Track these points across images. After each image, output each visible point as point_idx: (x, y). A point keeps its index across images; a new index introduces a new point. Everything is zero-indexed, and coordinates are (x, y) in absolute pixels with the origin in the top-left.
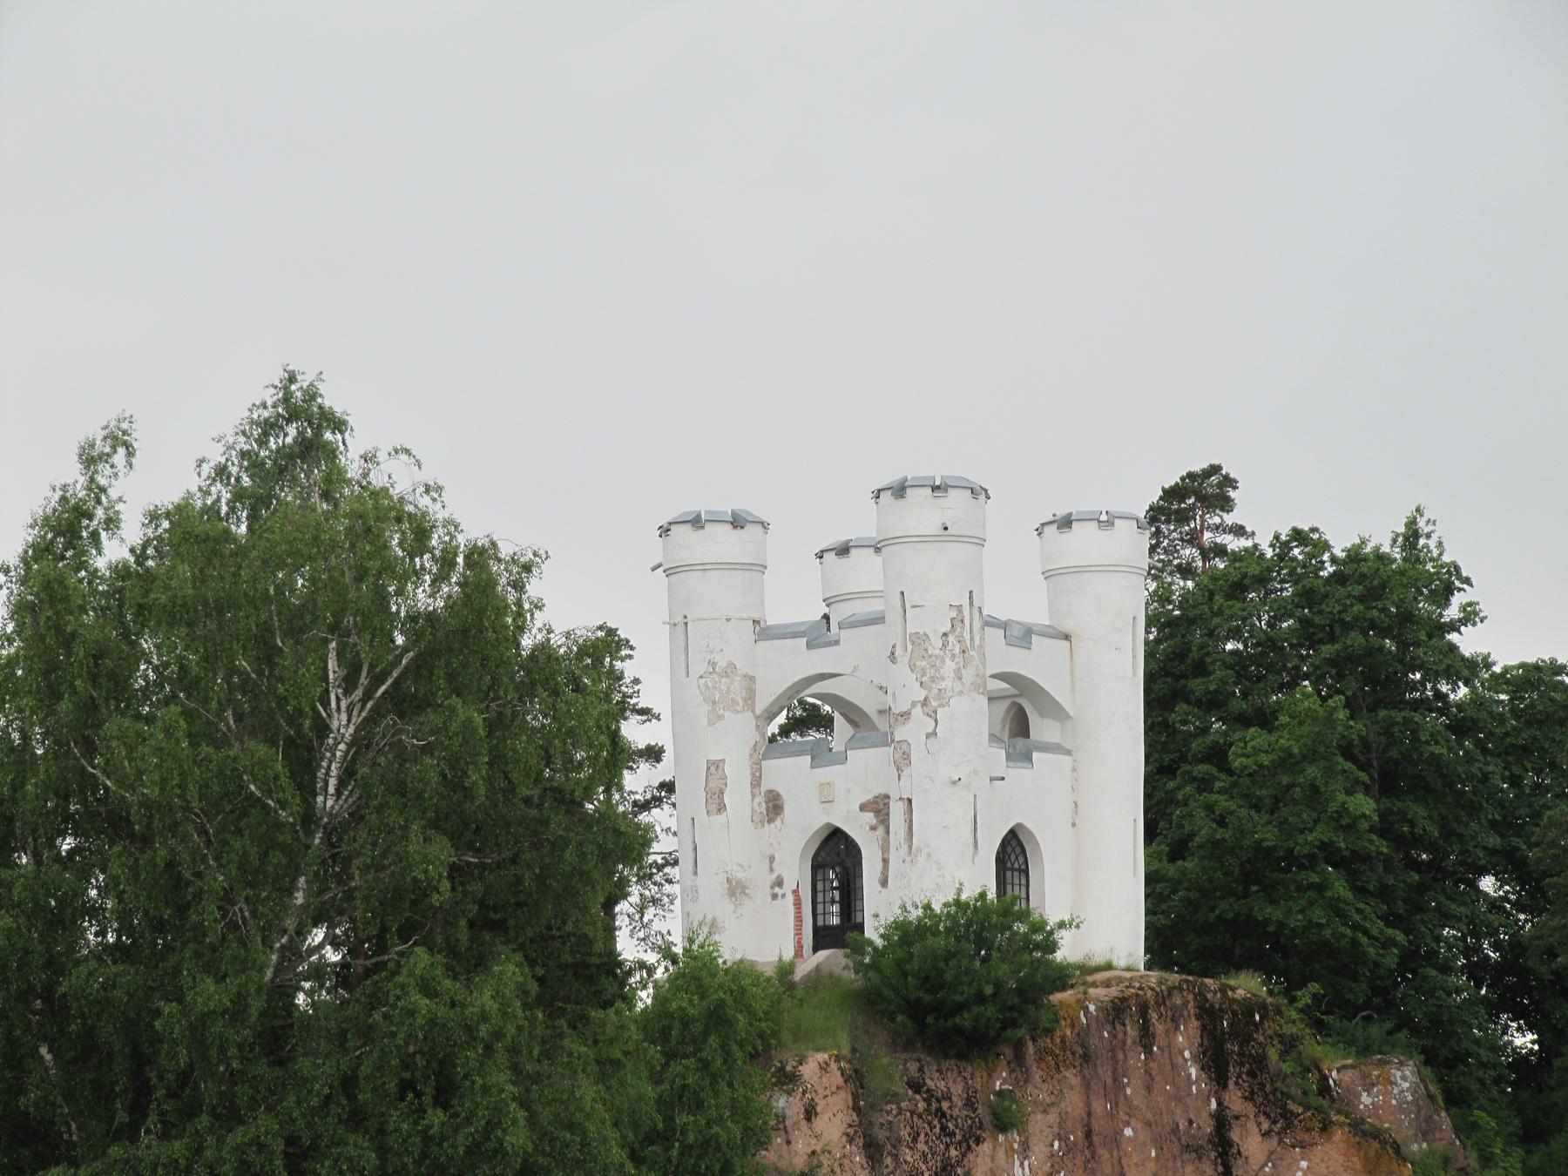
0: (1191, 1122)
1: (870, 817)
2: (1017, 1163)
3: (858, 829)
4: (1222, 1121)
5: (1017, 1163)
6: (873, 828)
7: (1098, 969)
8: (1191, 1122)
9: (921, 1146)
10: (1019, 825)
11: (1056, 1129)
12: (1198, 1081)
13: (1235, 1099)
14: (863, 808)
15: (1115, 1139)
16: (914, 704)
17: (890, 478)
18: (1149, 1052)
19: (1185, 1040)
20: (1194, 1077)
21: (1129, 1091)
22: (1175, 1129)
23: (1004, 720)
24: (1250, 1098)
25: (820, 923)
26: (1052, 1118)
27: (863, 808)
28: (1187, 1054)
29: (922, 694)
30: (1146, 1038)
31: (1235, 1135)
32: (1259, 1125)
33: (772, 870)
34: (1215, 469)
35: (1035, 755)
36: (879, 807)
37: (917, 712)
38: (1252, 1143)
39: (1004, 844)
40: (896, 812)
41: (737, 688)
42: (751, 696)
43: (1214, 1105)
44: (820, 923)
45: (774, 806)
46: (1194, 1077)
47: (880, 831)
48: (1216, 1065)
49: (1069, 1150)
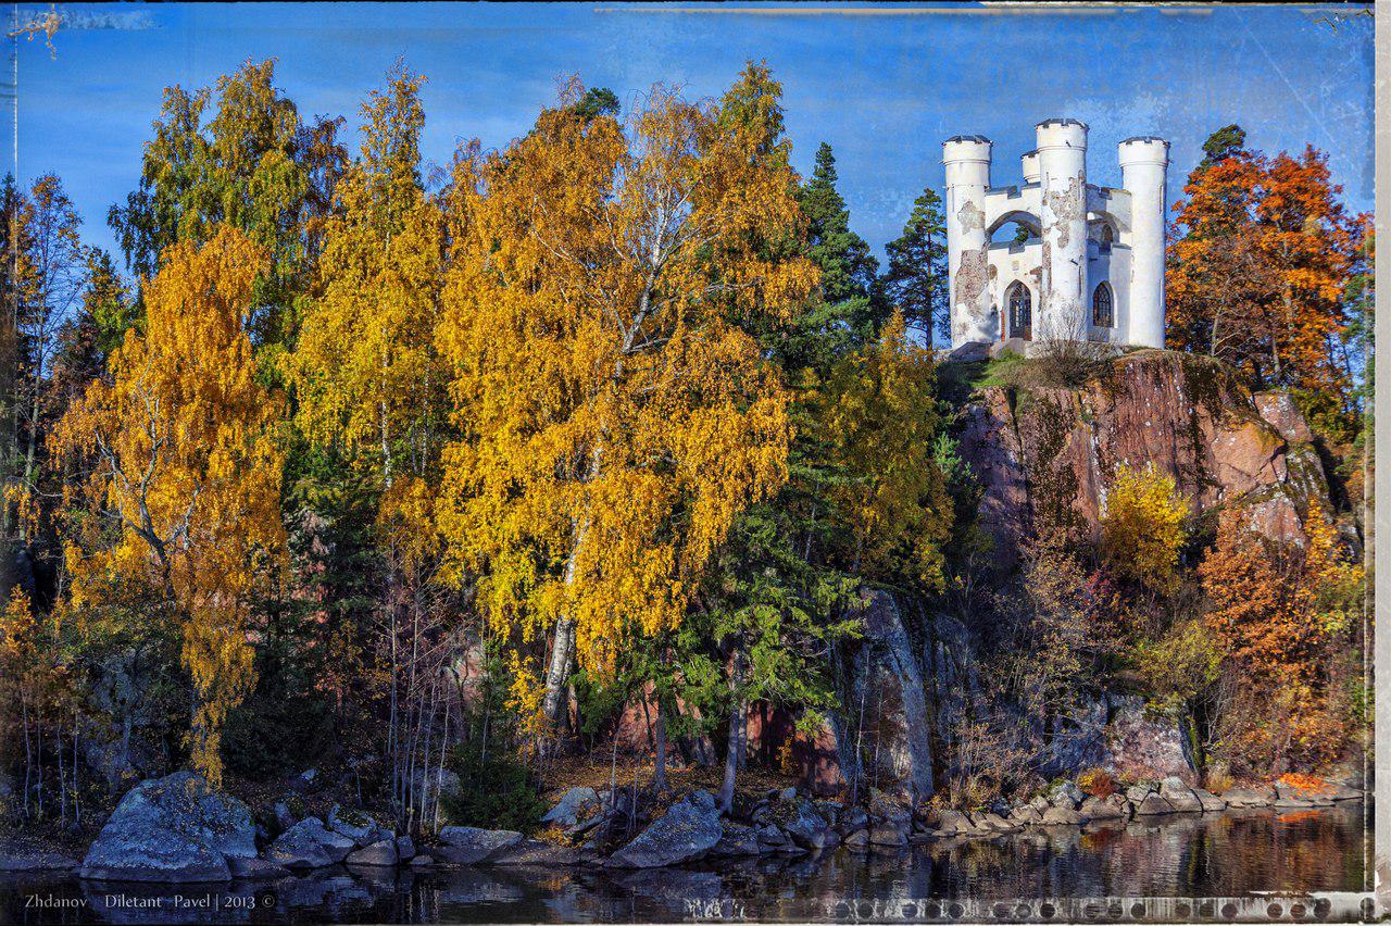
1: (1034, 277)
3: (1029, 281)
4: (1194, 418)
7: (1141, 348)
9: (1044, 428)
13: (1201, 410)
14: (1031, 272)
17: (1043, 120)
19: (1176, 381)
22: (1172, 424)
24: (1209, 409)
27: (1031, 272)
29: (1055, 220)
30: (1158, 380)
34: (1235, 128)
36: (1037, 272)
37: (1054, 228)
38: (1207, 427)
39: (1097, 290)
40: (1045, 273)
41: (976, 217)
42: (983, 220)
45: (993, 272)
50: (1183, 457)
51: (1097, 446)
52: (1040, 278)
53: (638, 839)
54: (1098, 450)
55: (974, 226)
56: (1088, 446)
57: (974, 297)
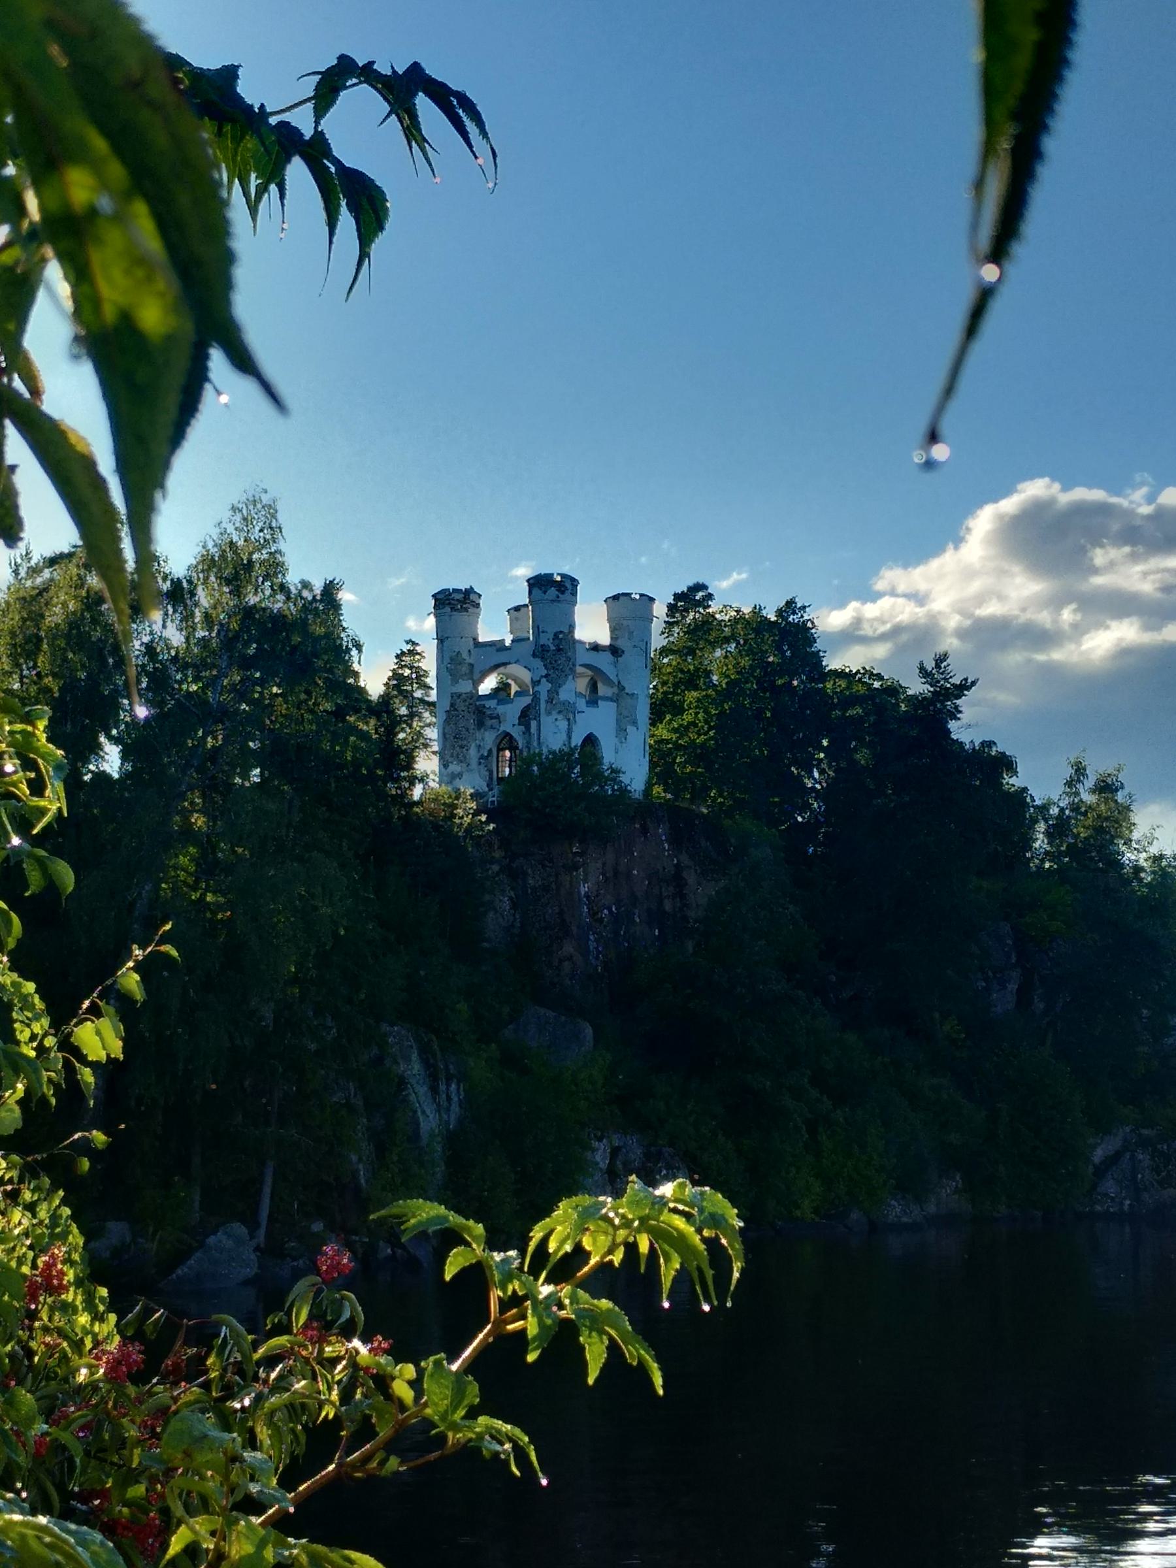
0: (664, 869)
2: (582, 885)
5: (582, 885)
6: (524, 733)
8: (664, 869)
10: (591, 733)
11: (601, 870)
12: (668, 850)
13: (685, 859)
15: (629, 875)
16: (542, 677)
18: (646, 837)
20: (667, 848)
21: (635, 854)
23: (587, 686)
25: (500, 776)
26: (599, 865)
28: (664, 838)
29: (545, 672)
30: (644, 830)
31: (685, 874)
32: (696, 870)
33: (479, 751)
35: (599, 702)
37: (544, 680)
41: (464, 669)
43: (675, 862)
44: (500, 776)
46: (667, 848)
47: (527, 736)
48: (676, 841)
49: (606, 880)
50: (668, 906)
51: (586, 893)
52: (528, 727)
53: (179, 1272)
54: (588, 897)
55: (462, 677)
56: (579, 892)
57: (462, 747)
